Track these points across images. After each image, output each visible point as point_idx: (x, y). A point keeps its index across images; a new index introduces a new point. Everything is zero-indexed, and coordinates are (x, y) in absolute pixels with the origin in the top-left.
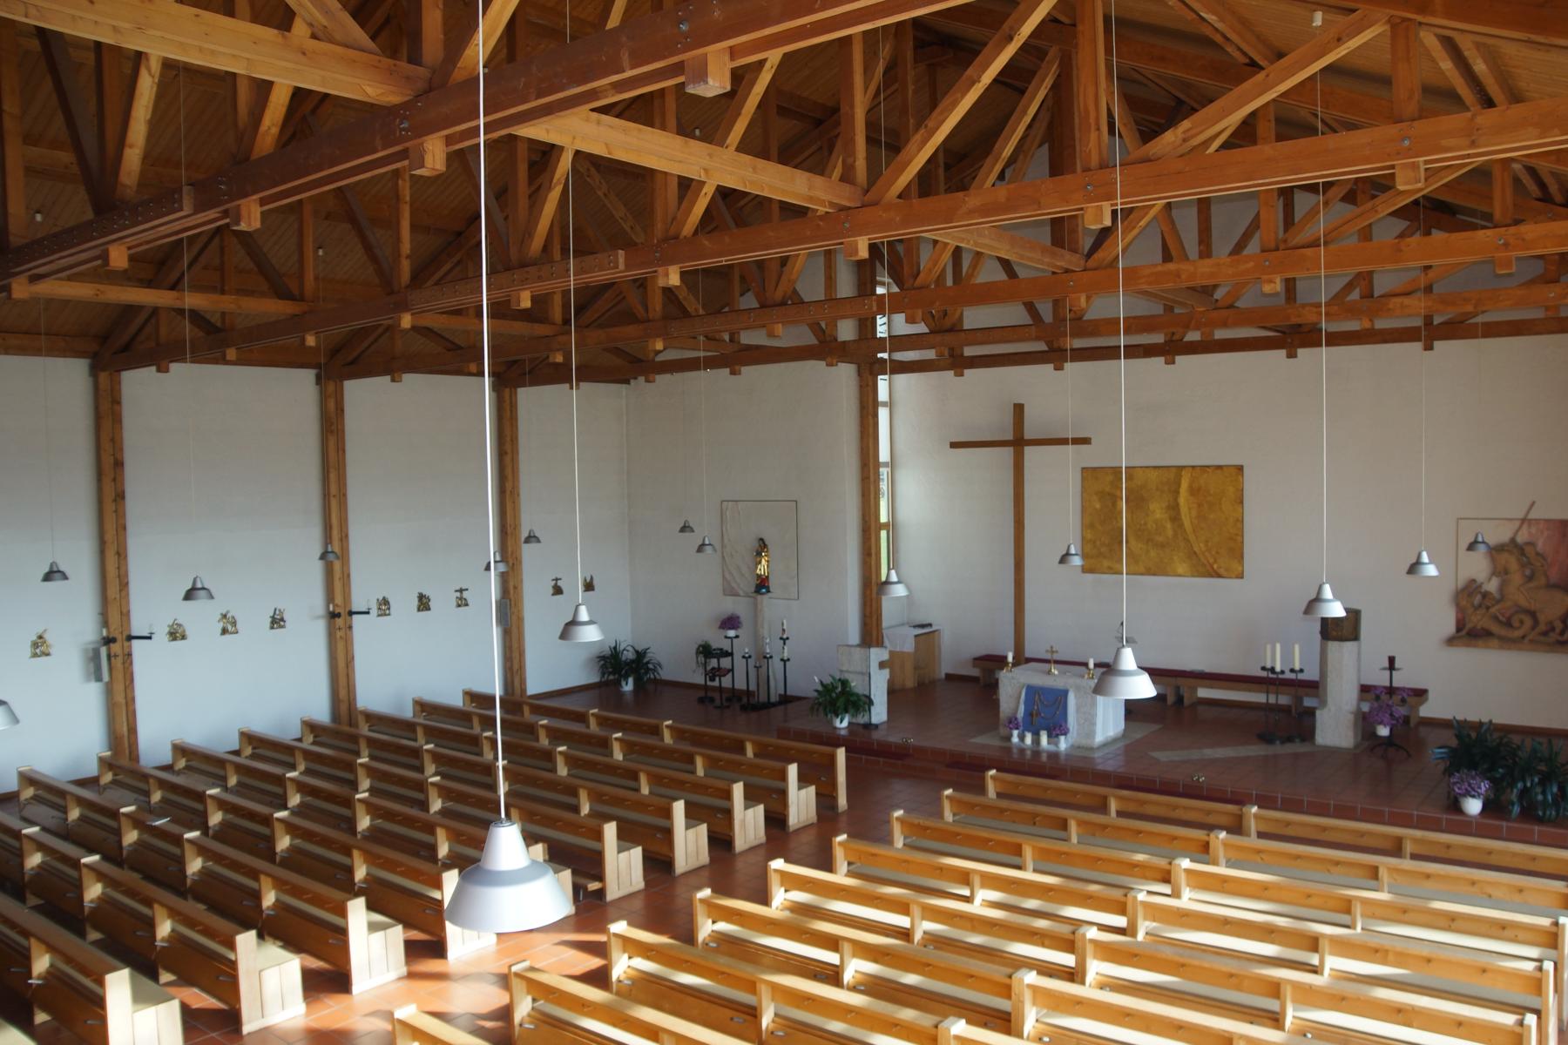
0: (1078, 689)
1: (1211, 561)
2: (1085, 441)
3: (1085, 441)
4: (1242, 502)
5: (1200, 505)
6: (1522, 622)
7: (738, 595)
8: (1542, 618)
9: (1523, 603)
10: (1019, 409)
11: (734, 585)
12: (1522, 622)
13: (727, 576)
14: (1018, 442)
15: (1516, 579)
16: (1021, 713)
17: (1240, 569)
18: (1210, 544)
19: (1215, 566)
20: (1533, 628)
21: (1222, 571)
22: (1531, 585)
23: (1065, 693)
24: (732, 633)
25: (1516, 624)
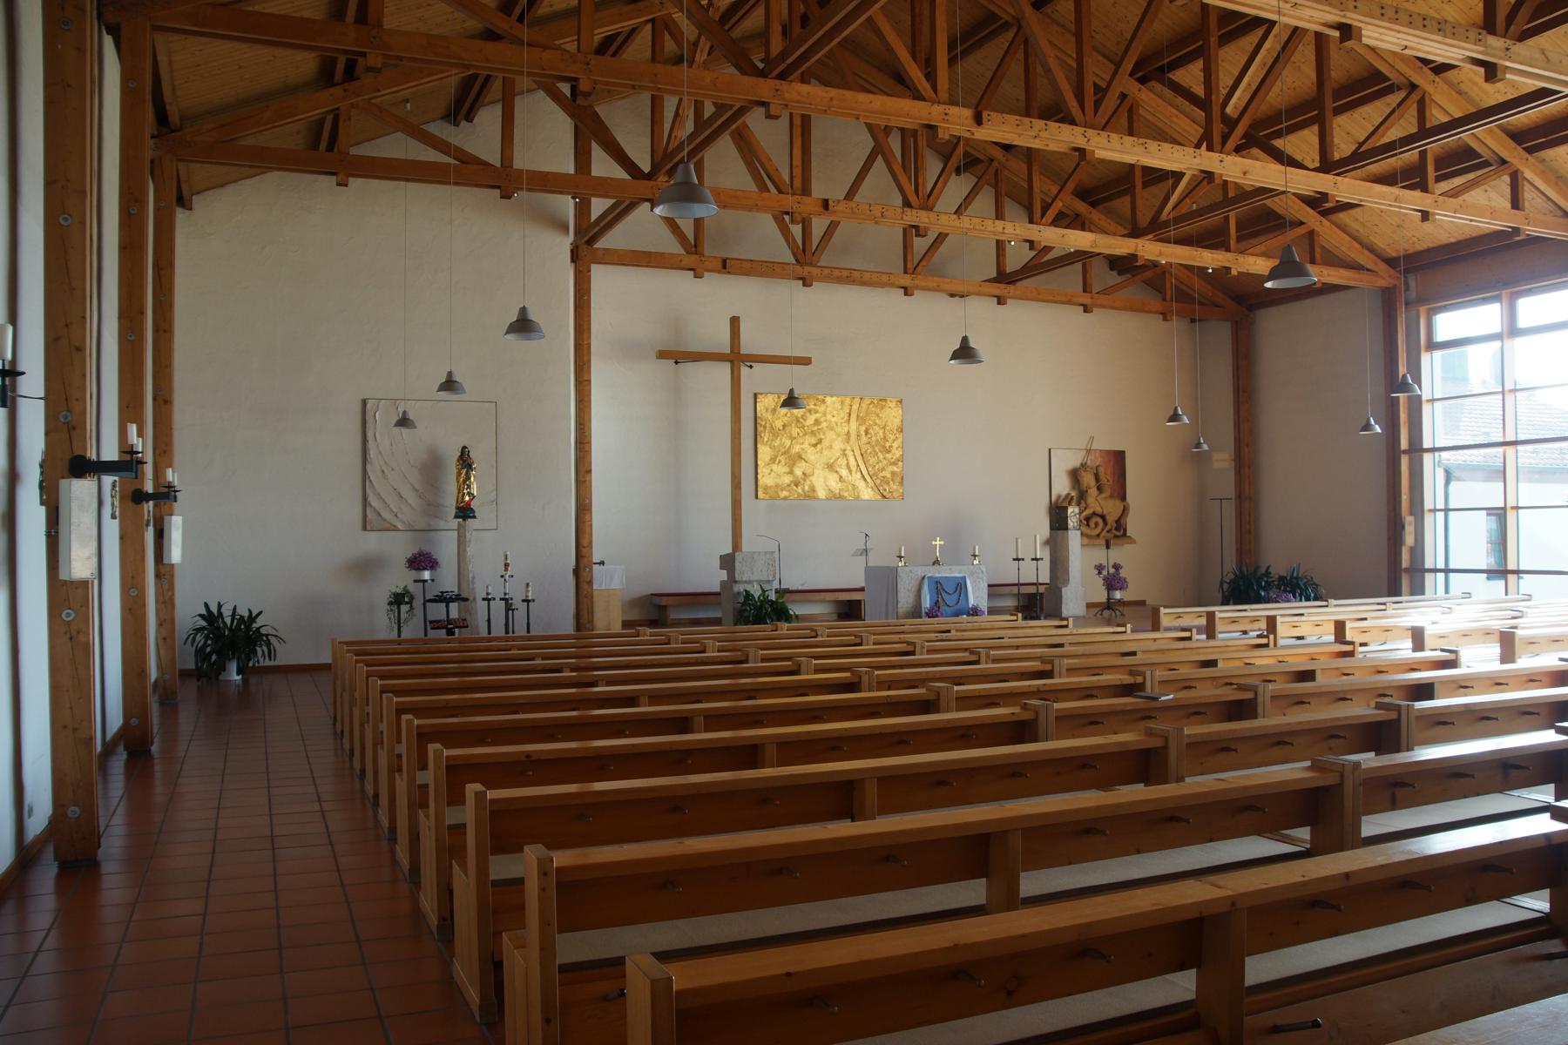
0: (972, 574)
1: (878, 482)
2: (806, 361)
3: (806, 361)
4: (902, 431)
5: (867, 432)
6: (1097, 524)
7: (396, 529)
8: (1111, 519)
9: (1099, 510)
10: (735, 322)
11: (385, 514)
12: (1097, 524)
13: (372, 499)
14: (736, 358)
15: (1093, 491)
16: (927, 603)
17: (901, 491)
18: (877, 467)
19: (881, 488)
20: (1103, 530)
21: (888, 495)
22: (1103, 495)
23: (964, 579)
24: (426, 575)
25: (1092, 524)
